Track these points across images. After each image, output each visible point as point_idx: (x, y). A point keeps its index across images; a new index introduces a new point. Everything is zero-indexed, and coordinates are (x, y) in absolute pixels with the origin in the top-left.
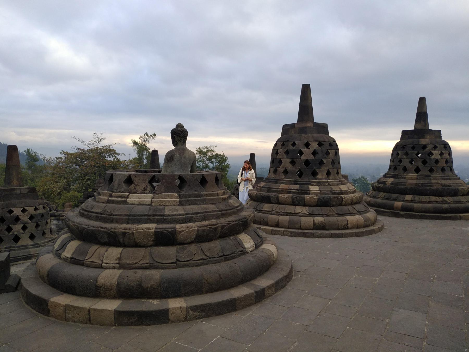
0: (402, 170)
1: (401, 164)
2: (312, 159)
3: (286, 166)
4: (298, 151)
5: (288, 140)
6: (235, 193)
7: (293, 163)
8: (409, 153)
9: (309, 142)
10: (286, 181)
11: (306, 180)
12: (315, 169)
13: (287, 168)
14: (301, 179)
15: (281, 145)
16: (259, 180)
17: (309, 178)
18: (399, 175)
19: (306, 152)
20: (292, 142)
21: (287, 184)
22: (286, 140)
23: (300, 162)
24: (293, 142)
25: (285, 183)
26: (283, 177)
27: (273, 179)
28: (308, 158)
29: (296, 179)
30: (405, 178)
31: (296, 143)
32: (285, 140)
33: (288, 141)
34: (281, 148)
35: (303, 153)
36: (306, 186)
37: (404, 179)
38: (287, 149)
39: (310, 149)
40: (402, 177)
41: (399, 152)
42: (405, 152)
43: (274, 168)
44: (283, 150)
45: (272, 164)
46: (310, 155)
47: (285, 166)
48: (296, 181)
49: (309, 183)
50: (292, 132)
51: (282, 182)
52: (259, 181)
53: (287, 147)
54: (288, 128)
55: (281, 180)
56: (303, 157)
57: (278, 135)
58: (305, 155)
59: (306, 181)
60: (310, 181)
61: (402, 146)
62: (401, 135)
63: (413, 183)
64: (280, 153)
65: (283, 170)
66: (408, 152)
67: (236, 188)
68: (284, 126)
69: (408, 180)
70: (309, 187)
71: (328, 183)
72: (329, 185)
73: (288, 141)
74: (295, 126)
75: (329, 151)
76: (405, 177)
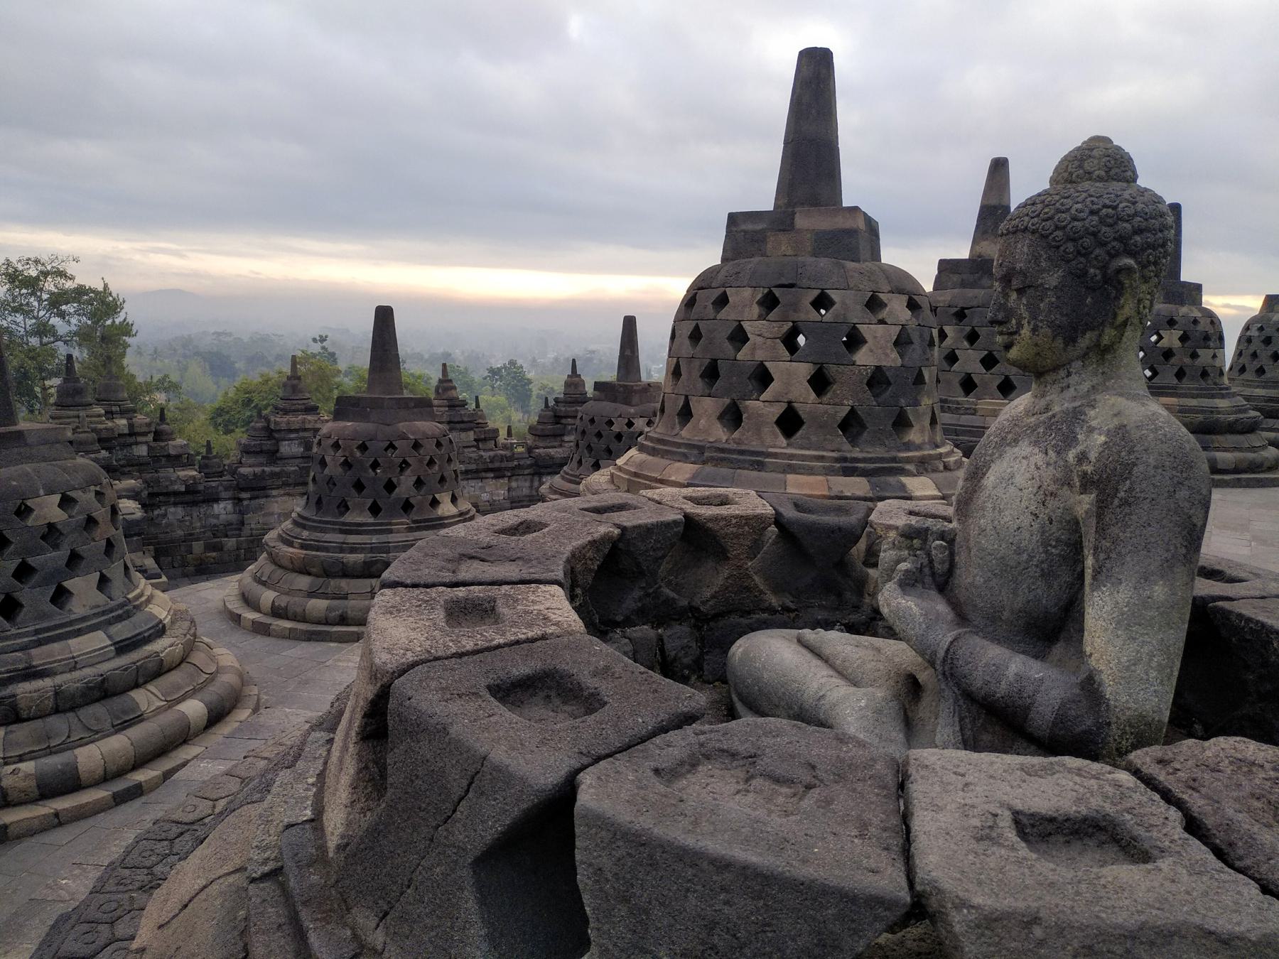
0: (958, 385)
1: (956, 366)
2: (896, 369)
3: (791, 397)
4: (846, 329)
5: (791, 282)
6: (328, 459)
7: (820, 382)
8: (983, 332)
9: (881, 295)
10: (804, 458)
11: (879, 452)
12: (902, 407)
13: (795, 405)
14: (861, 451)
15: (760, 303)
16: (415, 407)
17: (887, 443)
18: (953, 402)
19: (875, 337)
20: (817, 292)
21: (811, 472)
22: (786, 283)
23: (854, 377)
24: (819, 291)
25: (800, 467)
26: (779, 443)
27: (726, 446)
28: (884, 364)
29: (839, 451)
30: (974, 412)
31: (834, 295)
32: (780, 282)
33: (792, 286)
34: (761, 317)
35: (866, 342)
36: (891, 479)
37: (973, 414)
38: (793, 322)
39: (886, 323)
40: (967, 409)
41: (947, 329)
42: (968, 329)
43: (727, 401)
44: (774, 324)
45: (670, 374)
46: (889, 351)
47: (786, 394)
48: (845, 459)
49: (897, 469)
50: (783, 248)
51: (789, 465)
52: (415, 410)
53: (795, 311)
54: (759, 227)
55: (775, 455)
56: (864, 358)
57: (712, 256)
58: (871, 351)
59: (882, 460)
60: (894, 460)
61: (954, 310)
62: (937, 272)
63: (973, 427)
64: (760, 339)
65: (778, 410)
66: (976, 329)
67: (331, 442)
68: (733, 219)
69: (987, 418)
70: (903, 486)
71: (944, 462)
72: (946, 468)
73: (792, 286)
74: (793, 223)
75: (863, 329)
76: (975, 409)
